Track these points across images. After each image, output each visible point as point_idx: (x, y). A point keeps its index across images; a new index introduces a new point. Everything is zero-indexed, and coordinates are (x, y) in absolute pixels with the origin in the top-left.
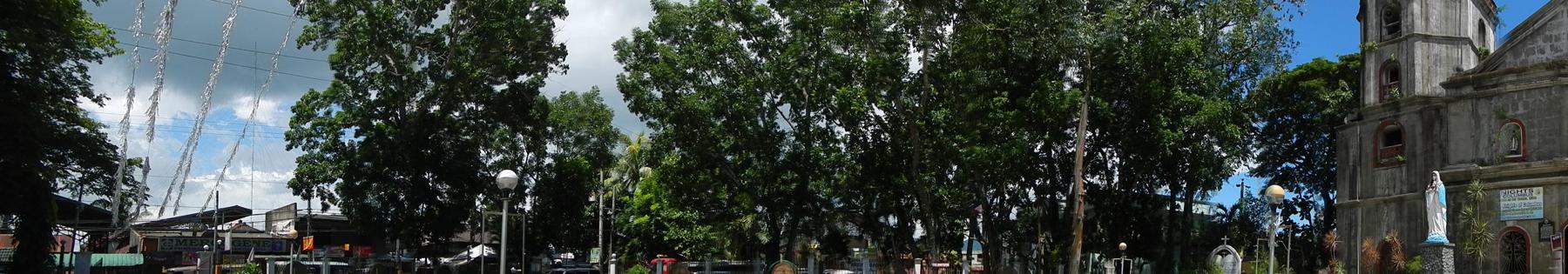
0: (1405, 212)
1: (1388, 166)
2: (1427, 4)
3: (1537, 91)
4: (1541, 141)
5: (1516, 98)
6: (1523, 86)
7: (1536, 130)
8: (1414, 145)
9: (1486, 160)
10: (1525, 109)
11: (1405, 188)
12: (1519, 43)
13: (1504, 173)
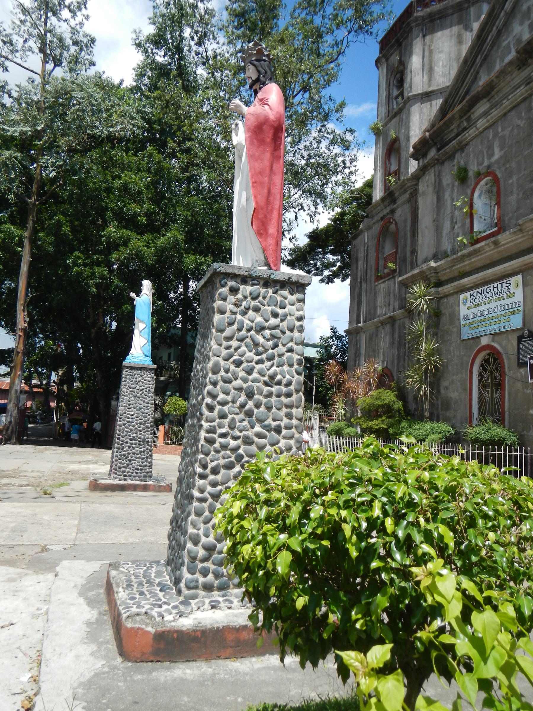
0: (396, 335)
1: (385, 277)
2: (431, 51)
3: (513, 113)
4: (520, 196)
5: (491, 137)
6: (496, 113)
7: (515, 178)
8: (405, 246)
9: (449, 250)
10: (501, 150)
11: (397, 304)
12: (492, 46)
13: (466, 265)
